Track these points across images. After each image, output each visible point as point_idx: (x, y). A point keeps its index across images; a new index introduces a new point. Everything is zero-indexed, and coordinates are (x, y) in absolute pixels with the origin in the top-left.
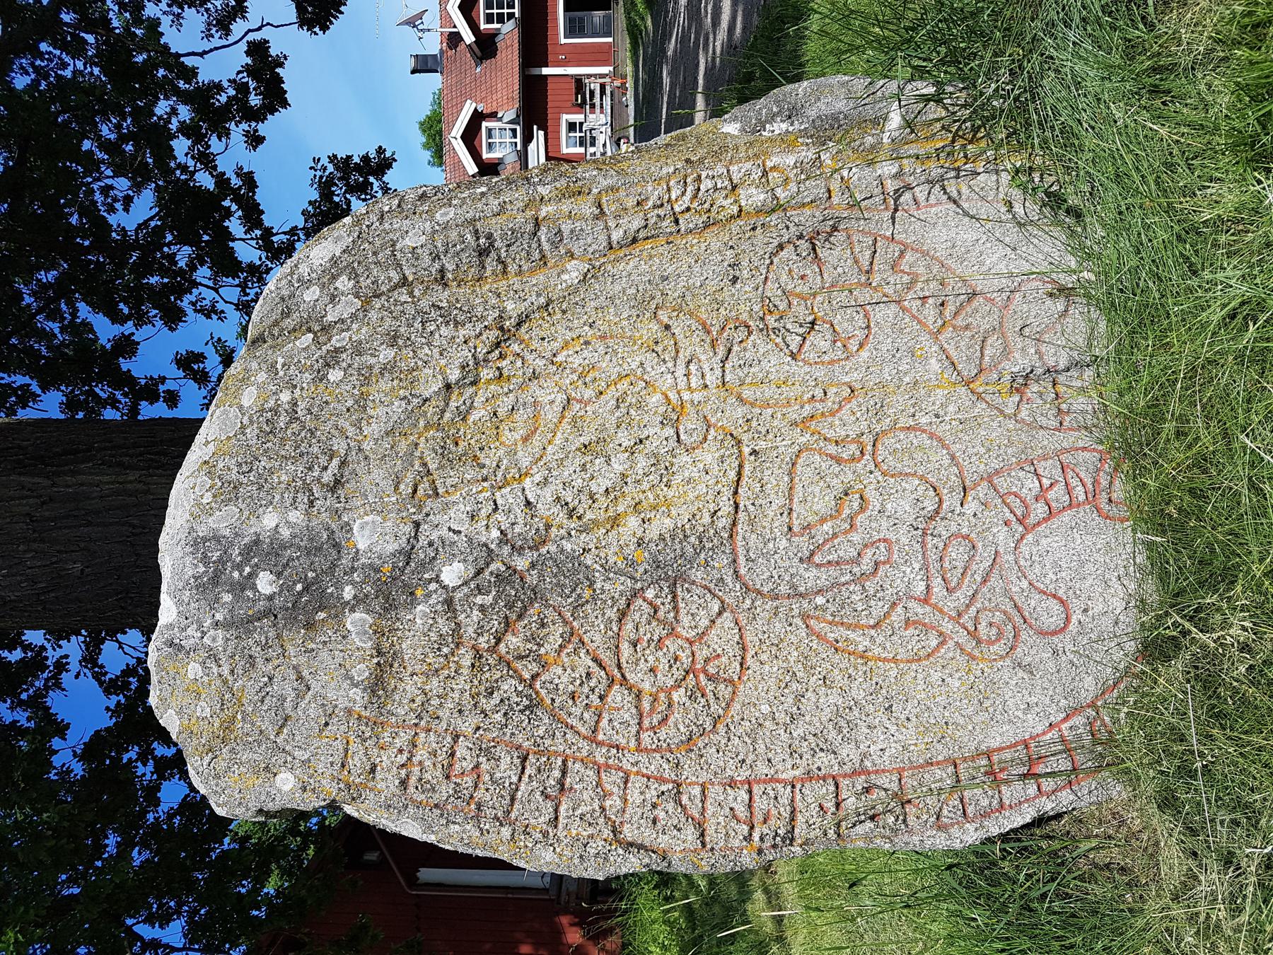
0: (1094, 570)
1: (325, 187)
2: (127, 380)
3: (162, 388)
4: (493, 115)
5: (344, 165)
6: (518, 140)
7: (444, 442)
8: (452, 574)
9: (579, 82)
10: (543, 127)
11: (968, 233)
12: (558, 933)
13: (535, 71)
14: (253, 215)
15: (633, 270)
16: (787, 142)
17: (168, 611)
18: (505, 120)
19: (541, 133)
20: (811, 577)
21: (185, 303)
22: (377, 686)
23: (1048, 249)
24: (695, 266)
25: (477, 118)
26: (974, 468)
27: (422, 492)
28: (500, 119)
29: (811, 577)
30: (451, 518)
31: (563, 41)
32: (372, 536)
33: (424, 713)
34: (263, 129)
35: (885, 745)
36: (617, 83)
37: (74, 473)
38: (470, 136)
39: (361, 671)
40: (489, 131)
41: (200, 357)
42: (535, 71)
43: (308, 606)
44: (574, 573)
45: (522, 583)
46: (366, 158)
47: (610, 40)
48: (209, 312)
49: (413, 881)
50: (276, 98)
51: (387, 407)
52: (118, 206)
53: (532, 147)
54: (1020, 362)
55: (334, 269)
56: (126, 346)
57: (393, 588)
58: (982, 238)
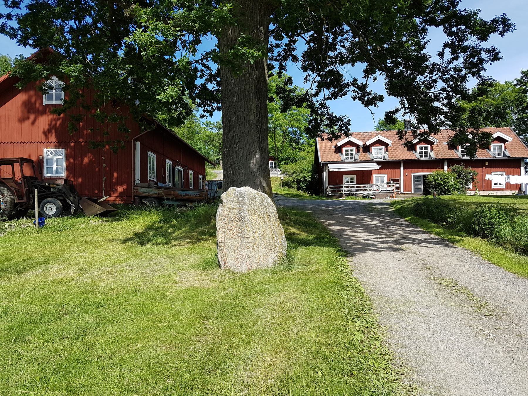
0: (243, 268)
1: (340, 119)
2: (285, 59)
3: (283, 71)
4: (387, 150)
5: (348, 123)
6: (378, 159)
7: (253, 213)
8: (242, 214)
9: (397, 181)
10: (380, 168)
11: (272, 258)
12: (121, 184)
13: (402, 165)
14: (334, 95)
15: (269, 229)
16: (280, 242)
17: (239, 189)
18: (385, 155)
19: (379, 168)
20: (242, 244)
21: (309, 72)
22: (233, 208)
23: (271, 265)
24: (269, 234)
25: (386, 145)
26: (251, 258)
27: (248, 211)
28: (385, 153)
29: (242, 244)
30: (246, 213)
31: (413, 175)
32: (245, 207)
33: (231, 212)
34: (357, 100)
35: (227, 250)
36: (394, 195)
37: (255, 98)
38: (379, 142)
39: (234, 207)
40: (382, 149)
41: (291, 85)
42: (402, 165)
43: (239, 202)
44: (242, 224)
45: (241, 219)
46: (349, 130)
47: (413, 192)
48: (306, 79)
49: (136, 140)
50: (367, 104)
51: (256, 208)
52: (342, 43)
53: (375, 164)
54: (261, 262)
55: (267, 203)
56: (295, 59)
57: (241, 209)
58: (272, 259)
